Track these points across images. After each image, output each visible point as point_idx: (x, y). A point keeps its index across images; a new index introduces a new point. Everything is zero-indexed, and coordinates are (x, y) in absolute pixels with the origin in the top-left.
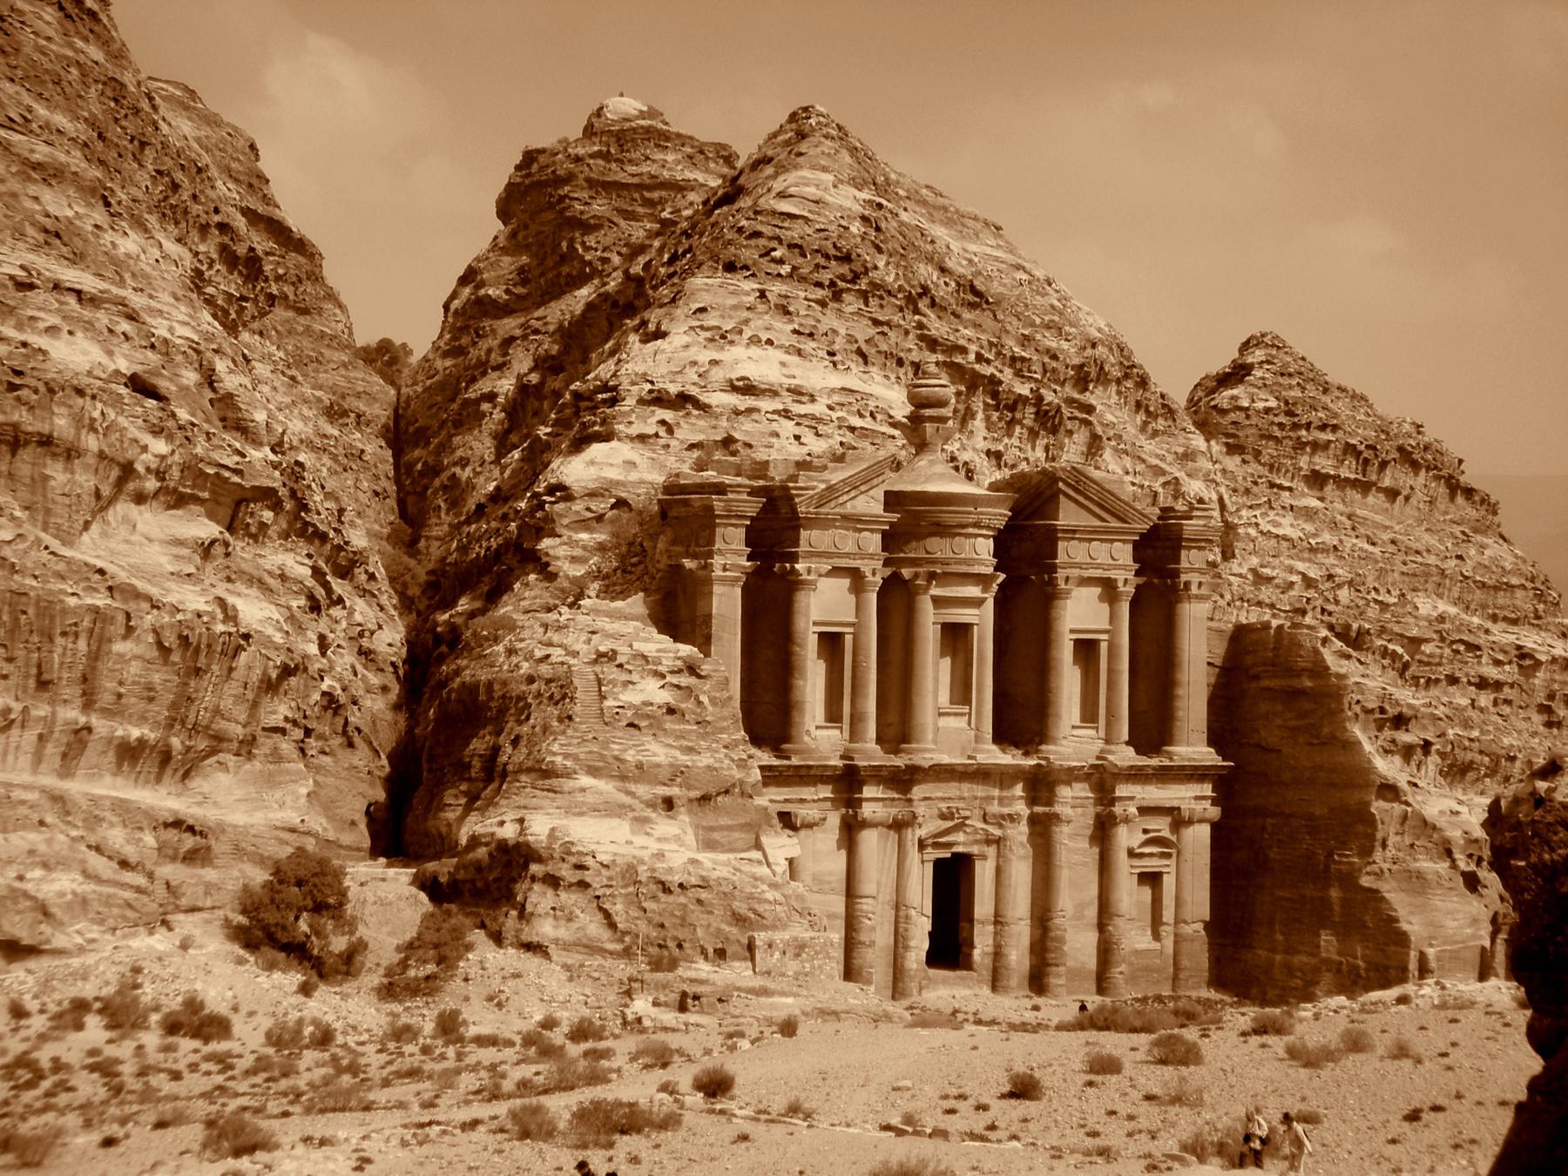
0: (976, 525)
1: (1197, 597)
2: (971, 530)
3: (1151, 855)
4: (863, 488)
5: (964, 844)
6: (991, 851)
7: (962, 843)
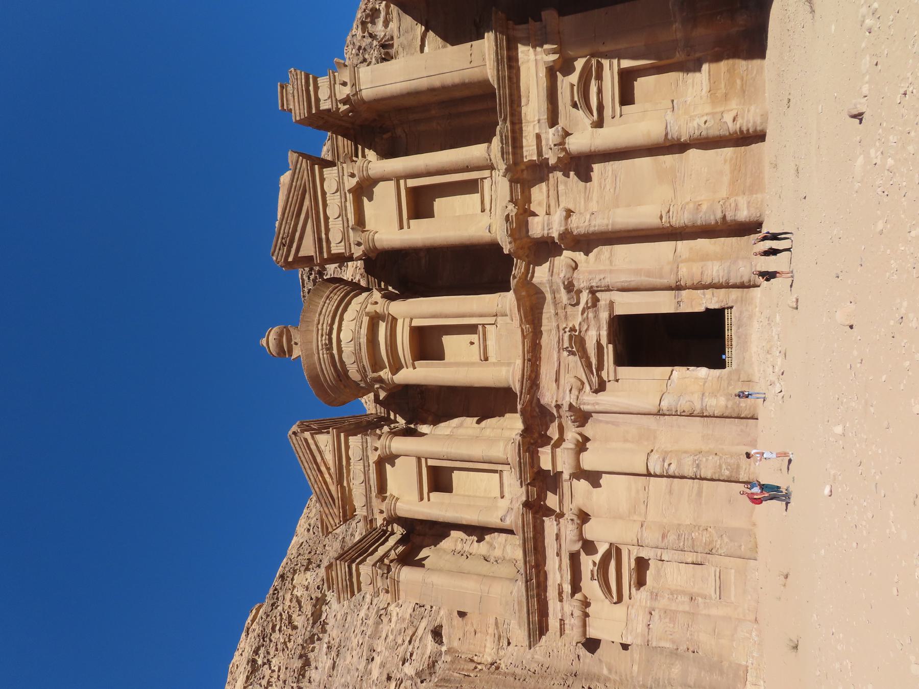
0: (329, 347)
1: (354, 85)
2: (335, 351)
3: (600, 91)
4: (319, 459)
5: (599, 329)
6: (604, 297)
7: (597, 333)
